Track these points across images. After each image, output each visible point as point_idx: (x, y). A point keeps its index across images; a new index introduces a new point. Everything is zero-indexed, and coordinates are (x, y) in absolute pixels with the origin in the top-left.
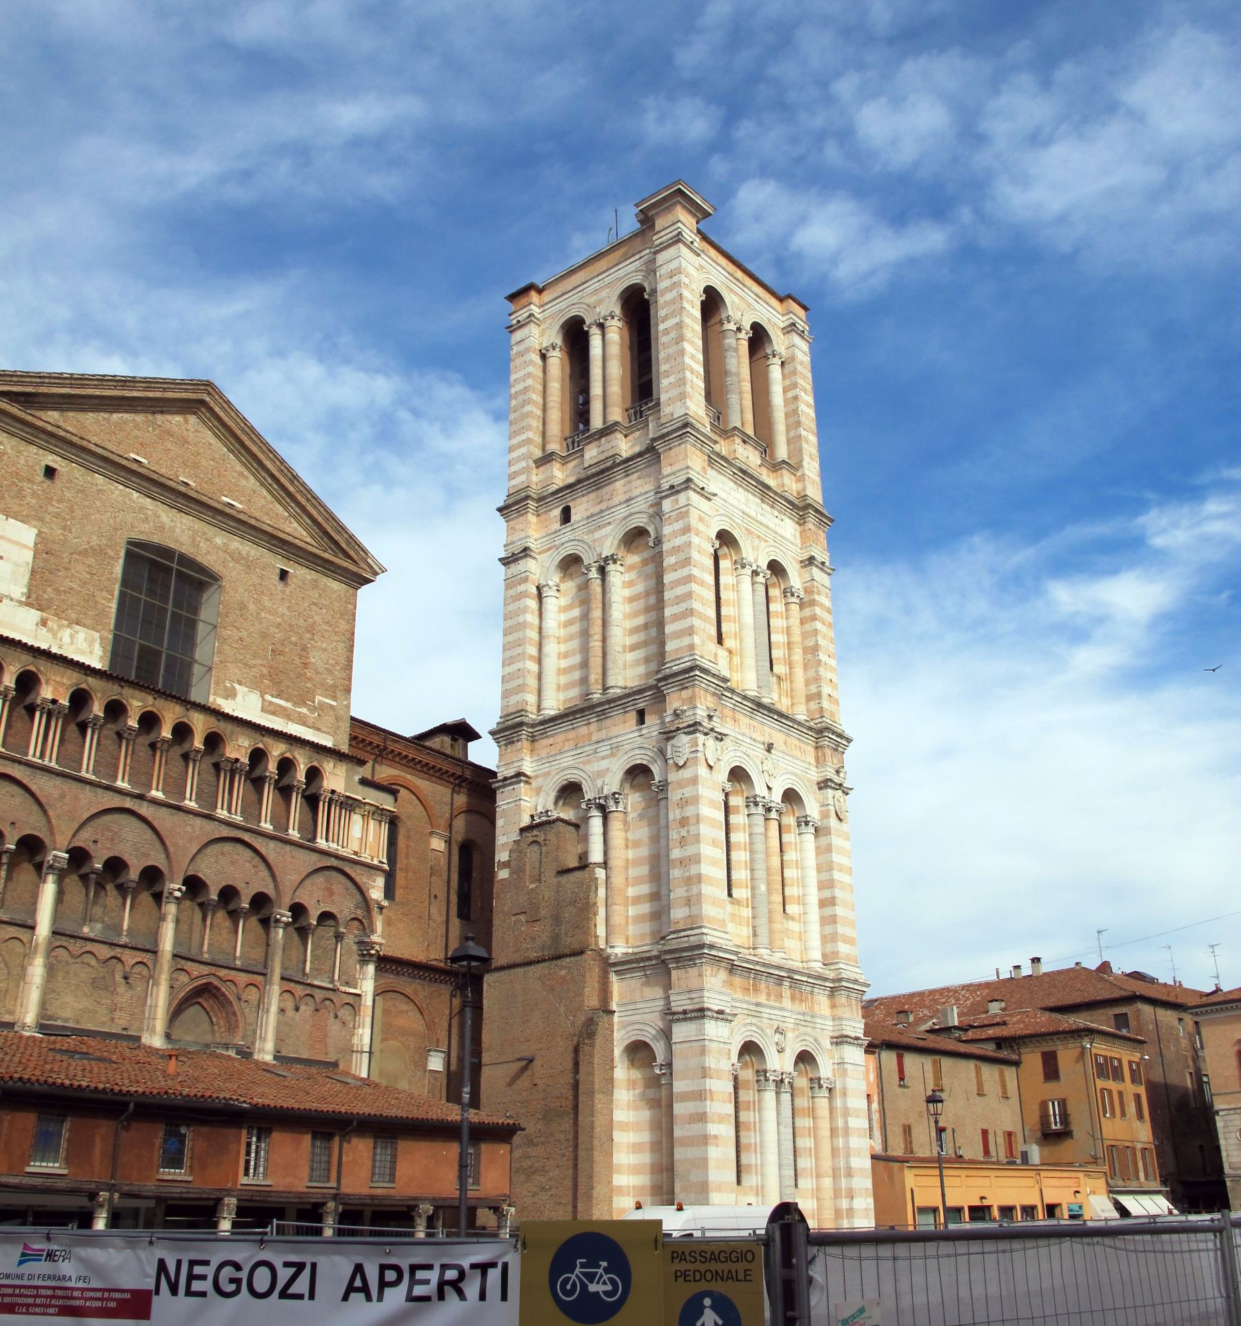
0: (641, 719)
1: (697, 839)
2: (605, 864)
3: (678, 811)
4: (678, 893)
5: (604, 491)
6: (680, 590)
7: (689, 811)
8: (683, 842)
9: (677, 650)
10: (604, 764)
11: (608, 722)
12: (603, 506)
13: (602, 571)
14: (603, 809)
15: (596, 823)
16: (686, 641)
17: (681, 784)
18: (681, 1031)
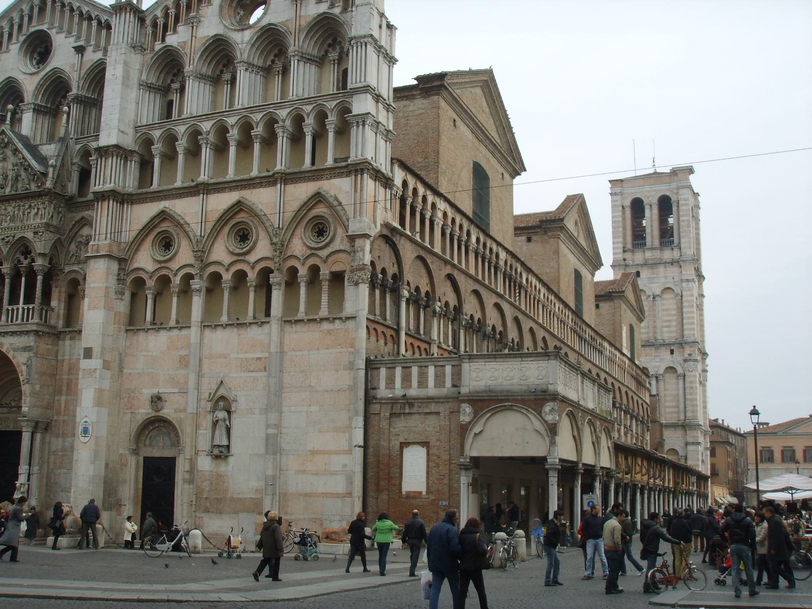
0: (672, 352)
1: (696, 394)
2: (658, 395)
3: (689, 384)
4: (689, 408)
5: (655, 270)
6: (690, 315)
7: (693, 385)
8: (691, 394)
9: (689, 334)
10: (658, 364)
11: (658, 351)
12: (655, 276)
13: (654, 298)
14: (657, 377)
15: (654, 382)
16: (692, 332)
17: (690, 377)
18: (690, 448)
